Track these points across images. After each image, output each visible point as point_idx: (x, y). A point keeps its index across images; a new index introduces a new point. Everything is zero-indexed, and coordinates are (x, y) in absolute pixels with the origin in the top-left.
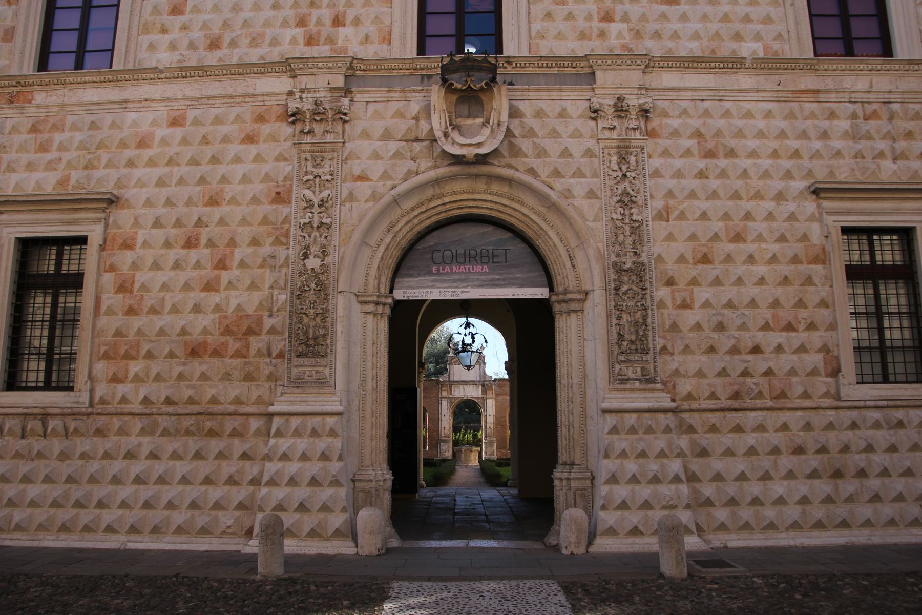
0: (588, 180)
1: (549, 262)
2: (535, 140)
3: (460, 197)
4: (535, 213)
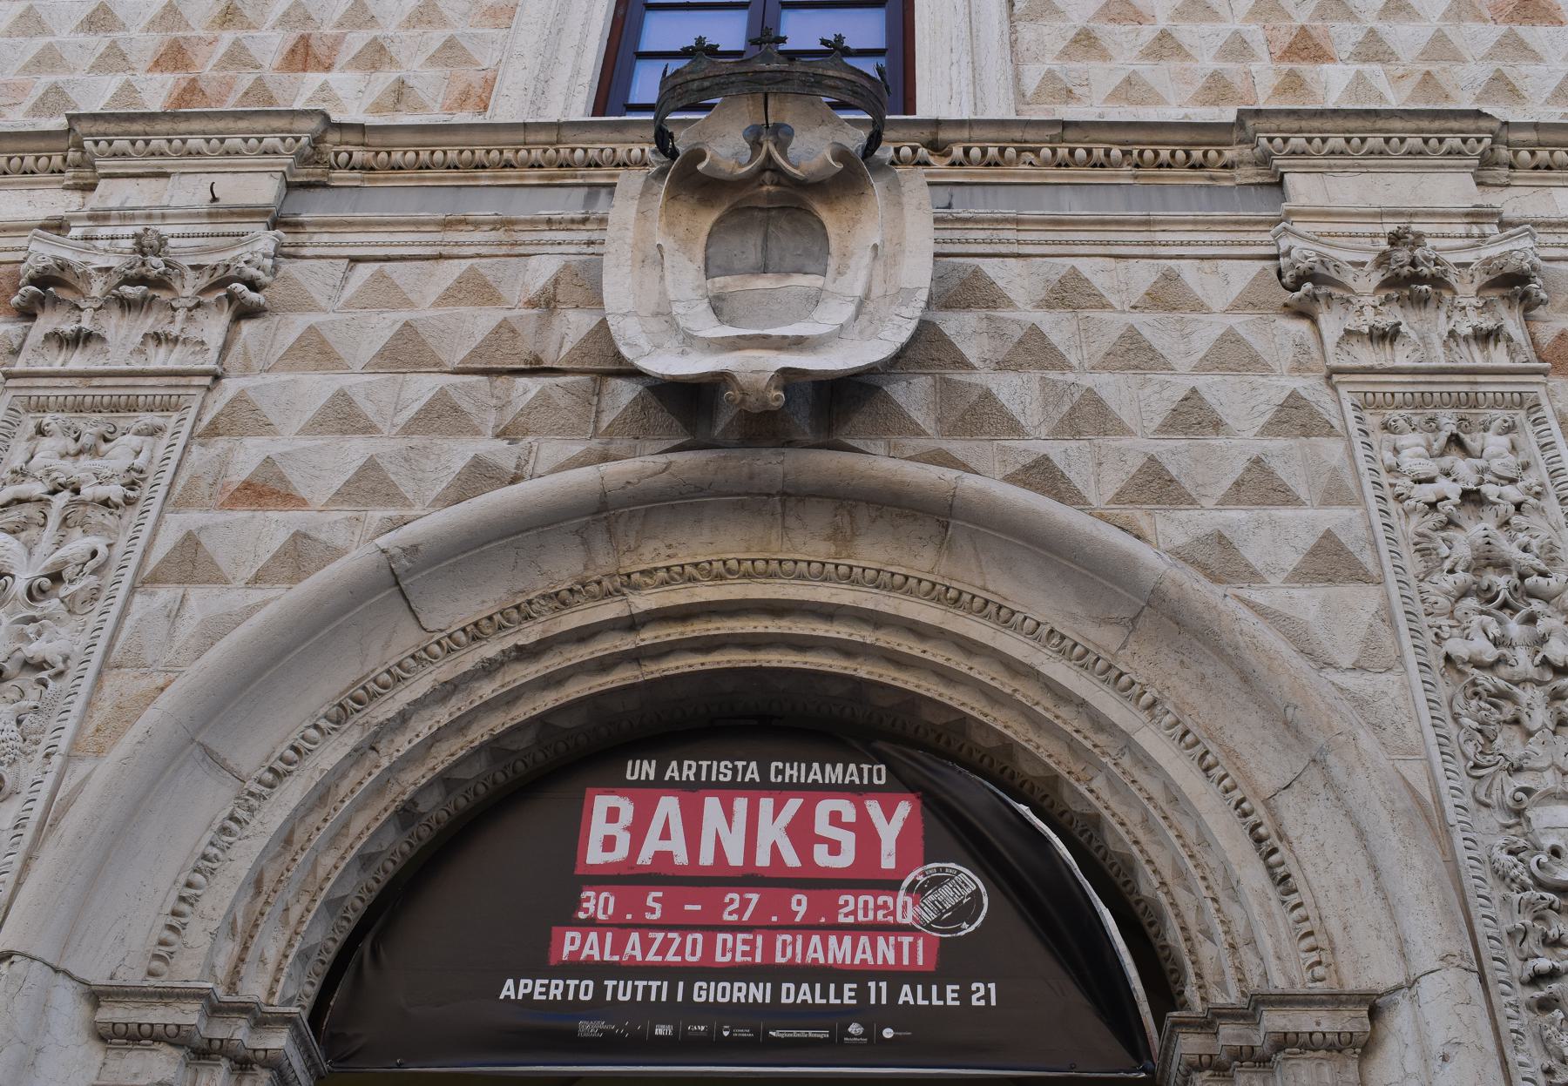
0: (1306, 513)
1: (1147, 885)
2: (1053, 375)
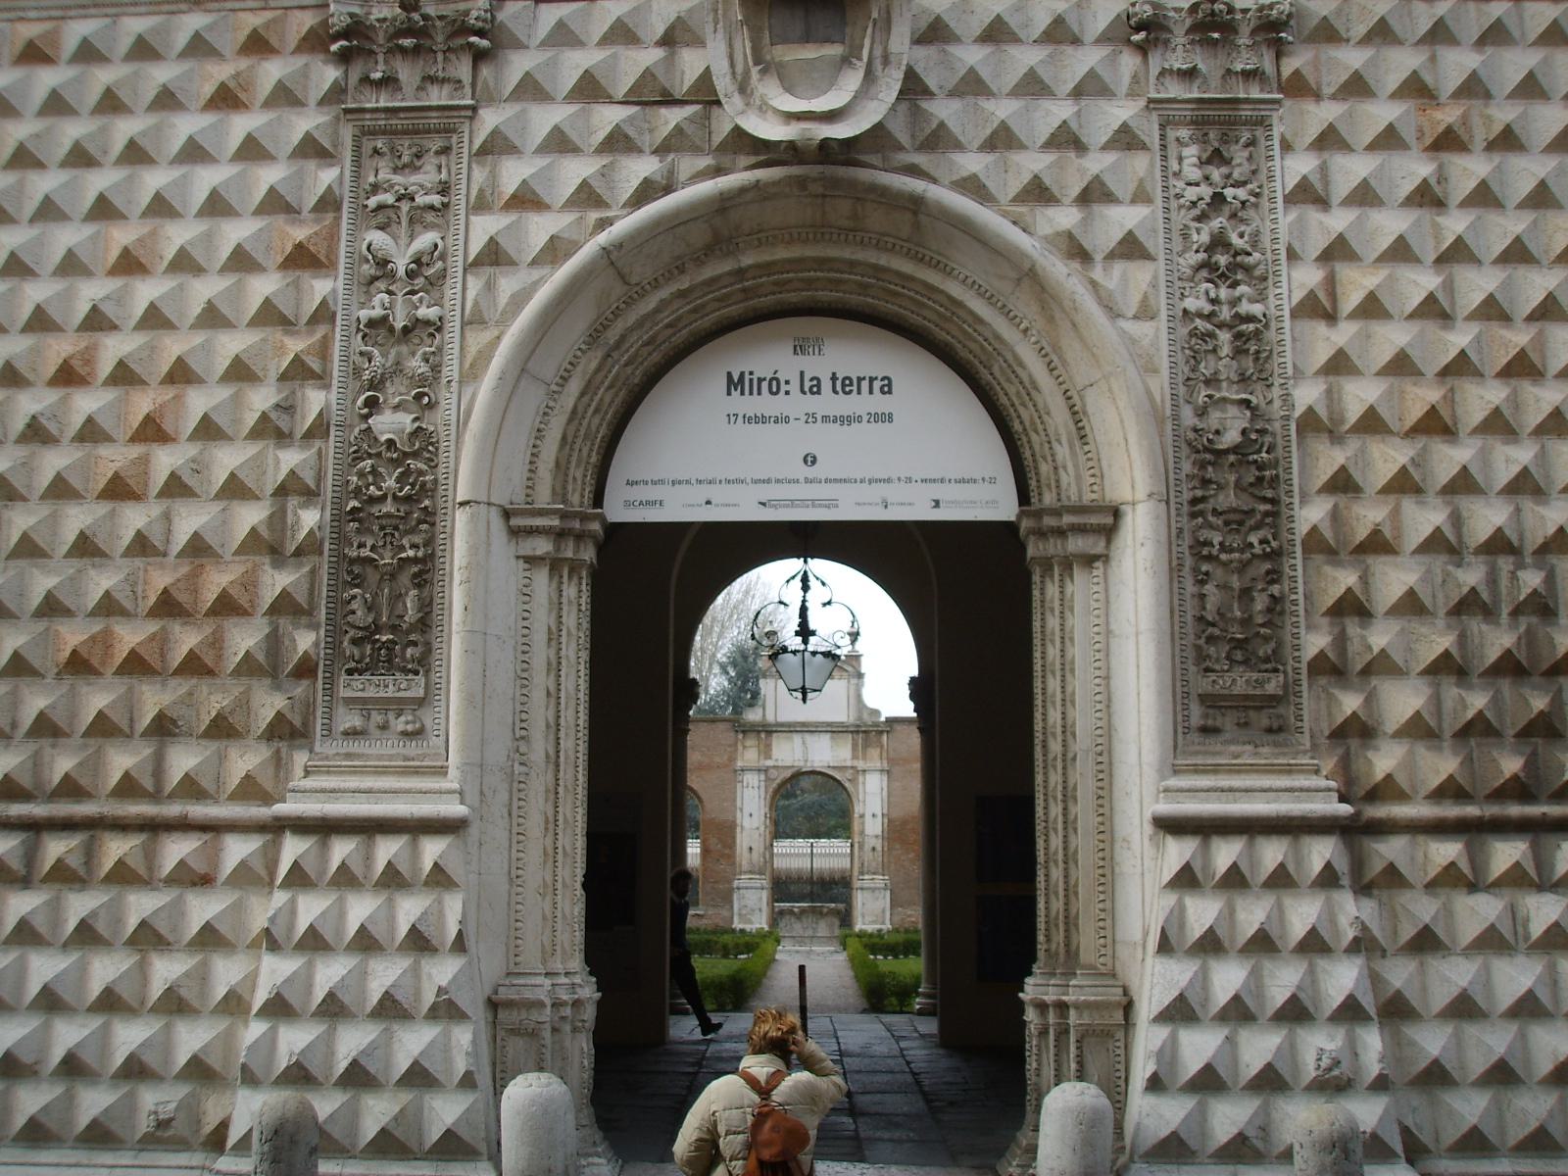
3: (781, 253)
4: (981, 295)
